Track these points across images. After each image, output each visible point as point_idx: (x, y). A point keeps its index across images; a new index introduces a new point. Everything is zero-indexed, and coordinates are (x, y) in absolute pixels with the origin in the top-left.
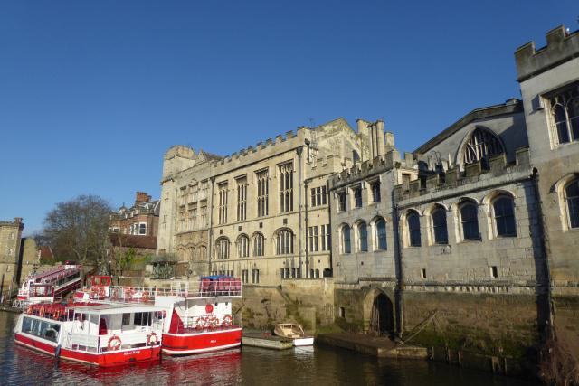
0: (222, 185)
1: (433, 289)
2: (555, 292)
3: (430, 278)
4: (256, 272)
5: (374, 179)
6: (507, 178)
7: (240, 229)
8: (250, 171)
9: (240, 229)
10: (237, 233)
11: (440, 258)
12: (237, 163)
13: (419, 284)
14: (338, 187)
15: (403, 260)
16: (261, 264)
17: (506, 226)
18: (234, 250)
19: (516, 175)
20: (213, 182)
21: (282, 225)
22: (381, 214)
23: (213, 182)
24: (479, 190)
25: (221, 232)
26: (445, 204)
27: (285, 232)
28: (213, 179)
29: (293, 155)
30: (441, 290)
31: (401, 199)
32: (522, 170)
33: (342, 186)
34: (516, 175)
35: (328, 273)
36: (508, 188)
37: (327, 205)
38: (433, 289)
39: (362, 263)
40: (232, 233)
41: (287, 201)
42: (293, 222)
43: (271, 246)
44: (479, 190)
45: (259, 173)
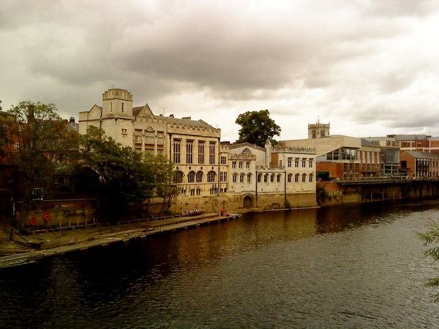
0: (179, 140)
4: (199, 190)
7: (190, 168)
8: (197, 139)
9: (190, 168)
10: (188, 171)
12: (189, 132)
16: (201, 187)
17: (278, 180)
18: (185, 178)
19: (282, 171)
20: (170, 136)
21: (211, 170)
23: (170, 136)
25: (177, 168)
27: (211, 174)
28: (170, 135)
29: (217, 140)
34: (282, 171)
35: (225, 189)
40: (186, 171)
41: (212, 161)
42: (216, 169)
43: (205, 178)
45: (200, 142)
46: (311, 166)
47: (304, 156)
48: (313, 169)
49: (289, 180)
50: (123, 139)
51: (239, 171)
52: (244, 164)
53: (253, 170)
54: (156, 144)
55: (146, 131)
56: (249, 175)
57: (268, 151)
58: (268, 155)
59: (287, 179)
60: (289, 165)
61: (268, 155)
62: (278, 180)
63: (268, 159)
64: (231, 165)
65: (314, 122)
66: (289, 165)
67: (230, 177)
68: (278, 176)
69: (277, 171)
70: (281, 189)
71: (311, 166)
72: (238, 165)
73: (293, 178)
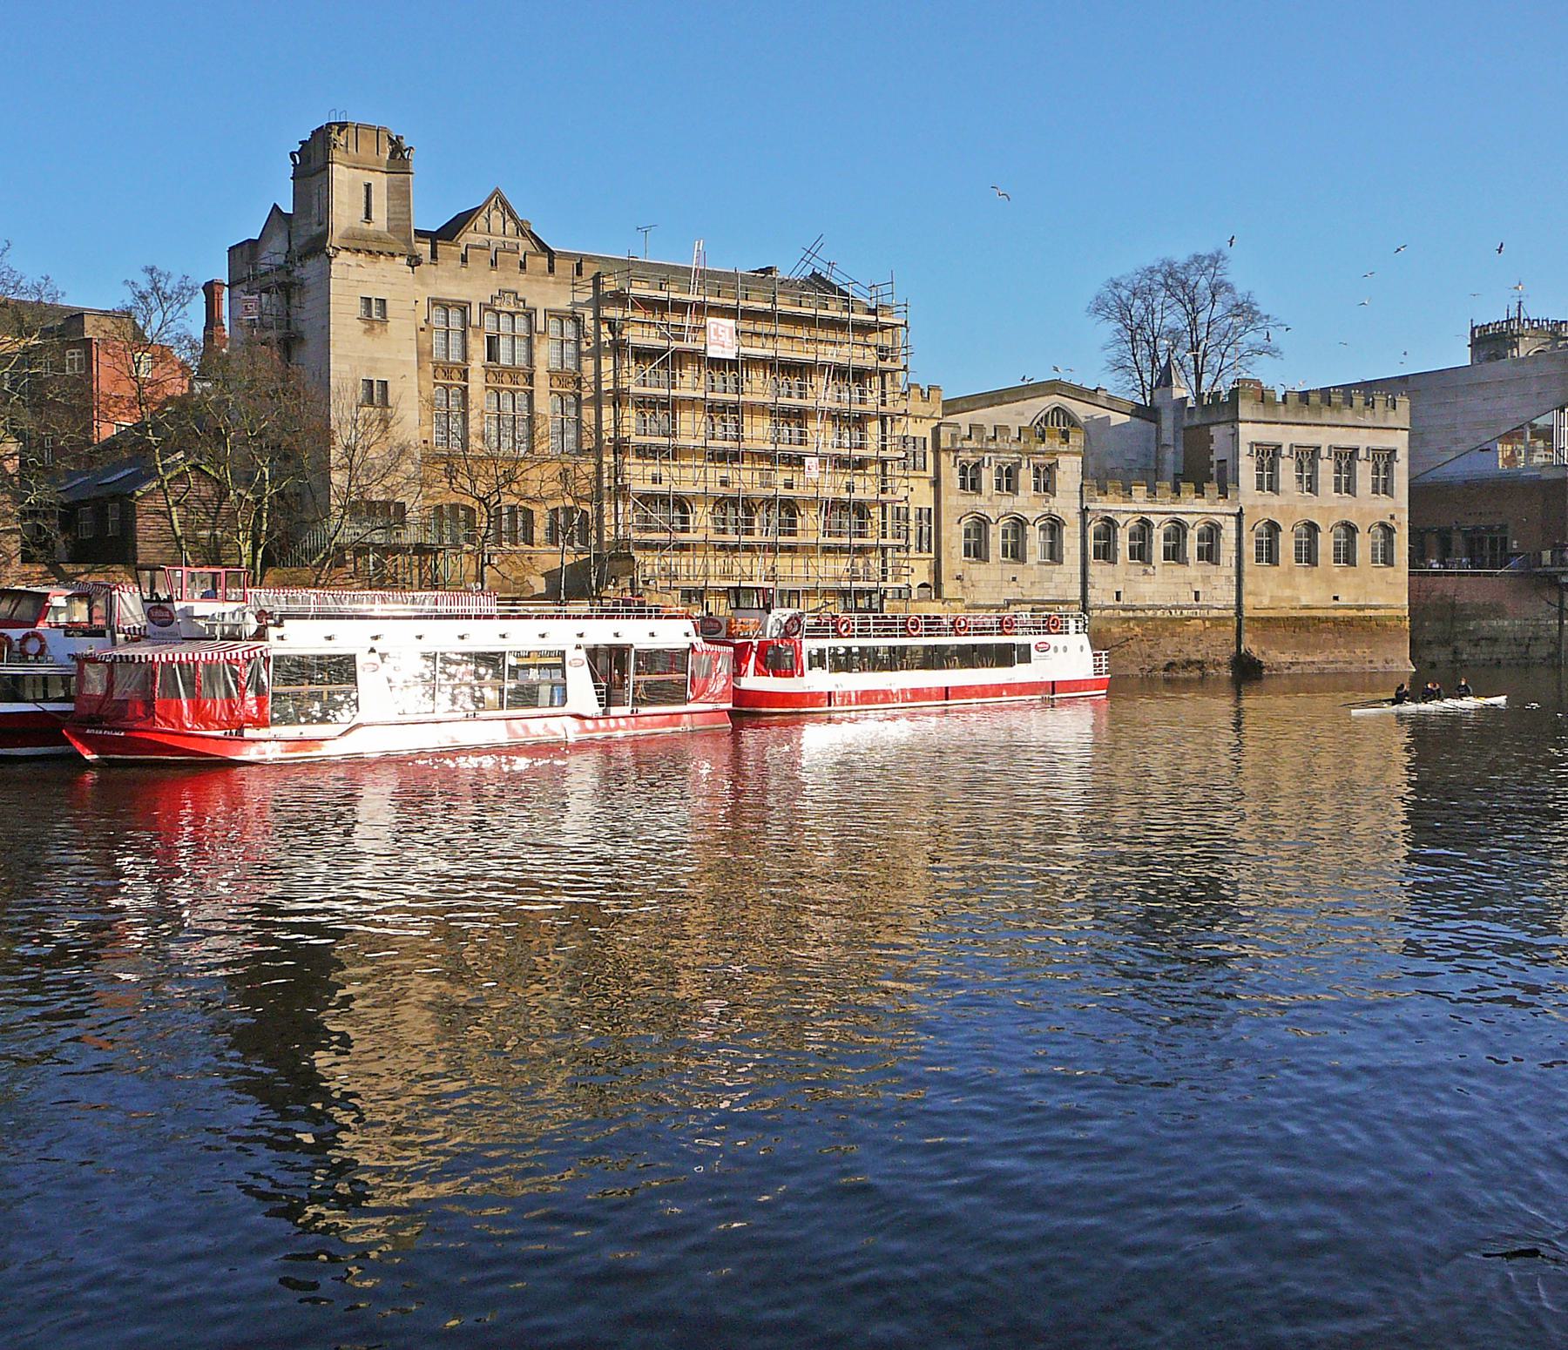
1: (1130, 614)
2: (1245, 614)
3: (1125, 601)
5: (1041, 460)
6: (1217, 509)
11: (1141, 579)
13: (1113, 608)
14: (963, 449)
15: (1090, 579)
22: (1054, 511)
24: (1193, 513)
26: (1152, 518)
30: (1139, 614)
31: (1095, 501)
32: (1232, 504)
33: (972, 450)
36: (1217, 518)
37: (930, 472)
38: (1130, 614)
39: (1014, 579)
44: (1193, 513)
46: (1384, 487)
47: (1345, 439)
48: (1397, 506)
49: (1269, 553)
50: (367, 340)
51: (993, 504)
52: (1026, 477)
53: (1065, 504)
54: (541, 371)
55: (486, 308)
56: (1054, 526)
57: (1167, 423)
58: (1167, 435)
59: (1250, 549)
60: (1269, 483)
61: (1167, 435)
62: (1209, 554)
63: (1169, 455)
64: (951, 477)
65: (1493, 314)
66: (1269, 483)
67: (954, 536)
68: (1211, 533)
69: (1195, 509)
70: (1221, 595)
71: (1384, 487)
72: (988, 477)
73: (1287, 544)
